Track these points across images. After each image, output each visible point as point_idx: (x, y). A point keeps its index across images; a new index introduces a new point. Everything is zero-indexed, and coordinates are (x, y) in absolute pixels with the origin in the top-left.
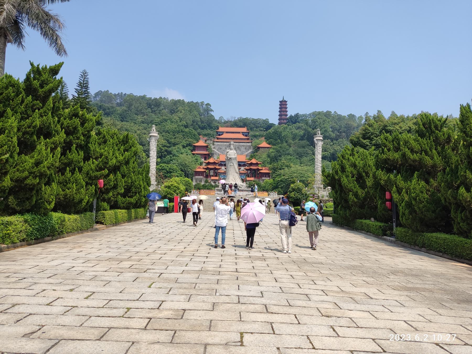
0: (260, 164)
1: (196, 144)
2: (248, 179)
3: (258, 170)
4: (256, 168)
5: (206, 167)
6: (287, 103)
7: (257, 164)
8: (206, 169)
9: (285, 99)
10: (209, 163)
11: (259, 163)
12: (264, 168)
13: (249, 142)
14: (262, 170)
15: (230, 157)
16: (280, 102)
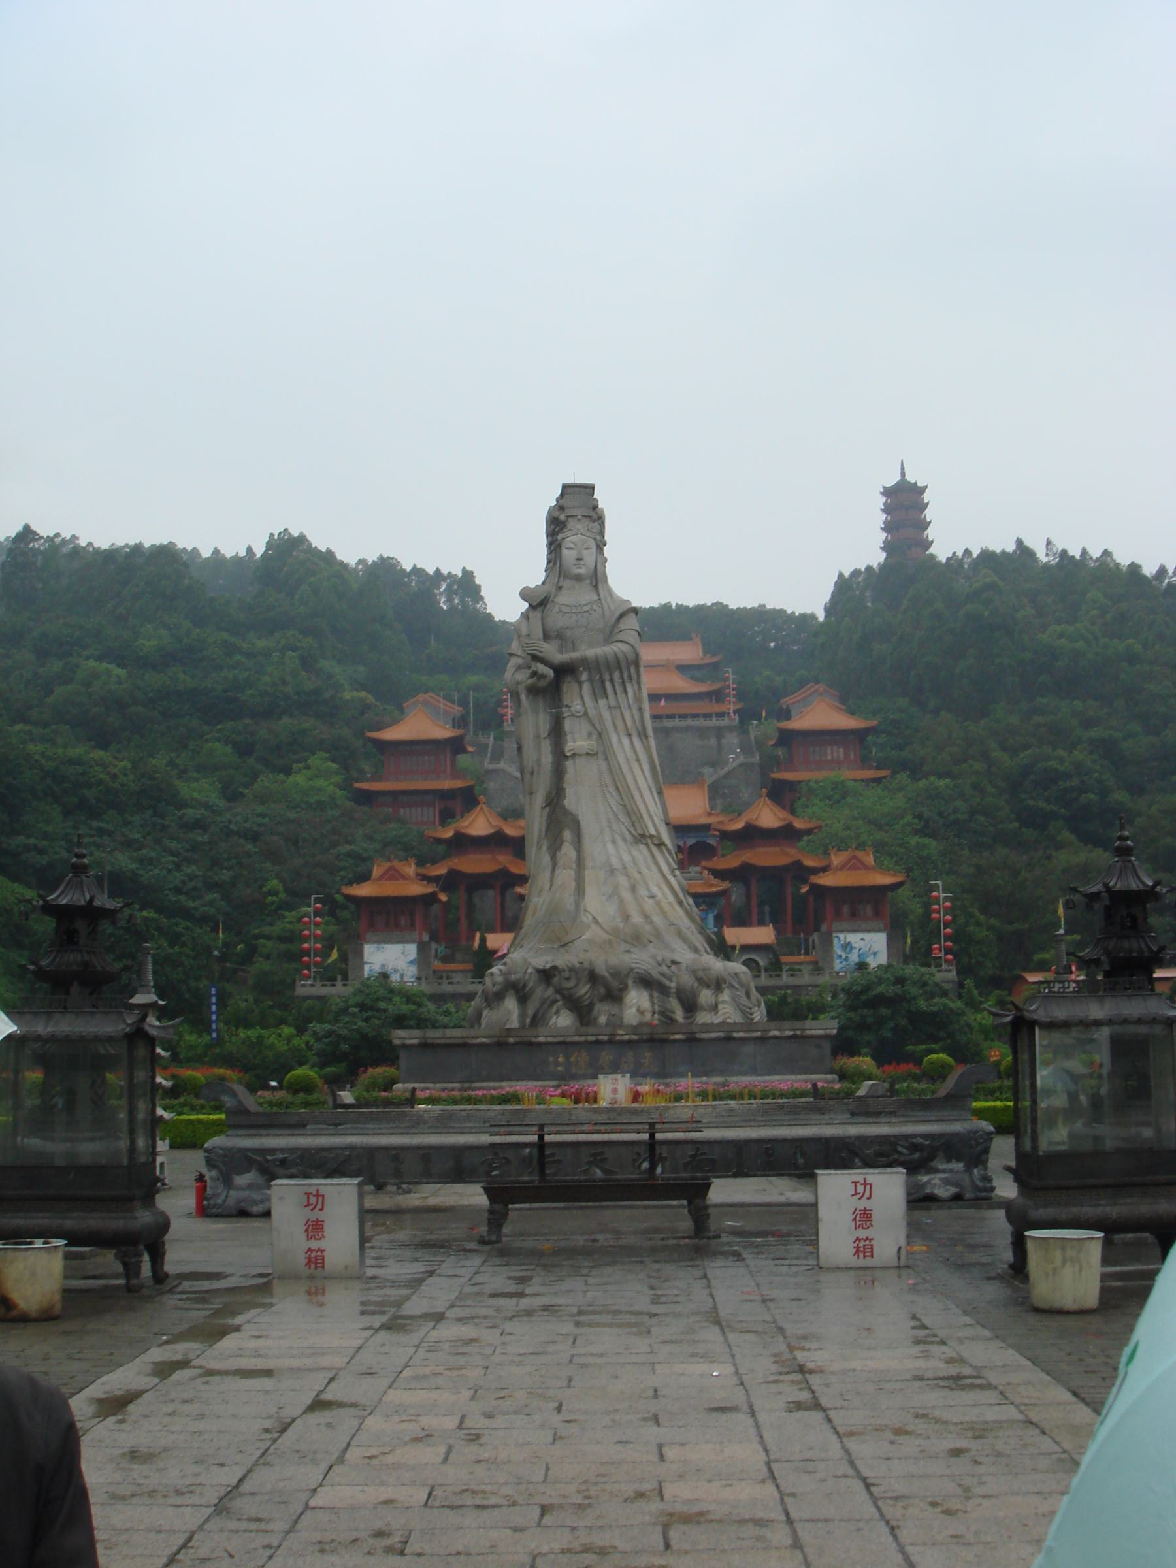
0: (809, 832)
1: (389, 735)
2: (735, 936)
3: (800, 872)
4: (783, 861)
5: (441, 870)
6: (927, 497)
7: (787, 834)
8: (451, 881)
9: (911, 478)
10: (462, 843)
11: (798, 824)
12: (836, 860)
13: (721, 715)
14: (824, 869)
15: (561, 658)
16: (887, 492)
